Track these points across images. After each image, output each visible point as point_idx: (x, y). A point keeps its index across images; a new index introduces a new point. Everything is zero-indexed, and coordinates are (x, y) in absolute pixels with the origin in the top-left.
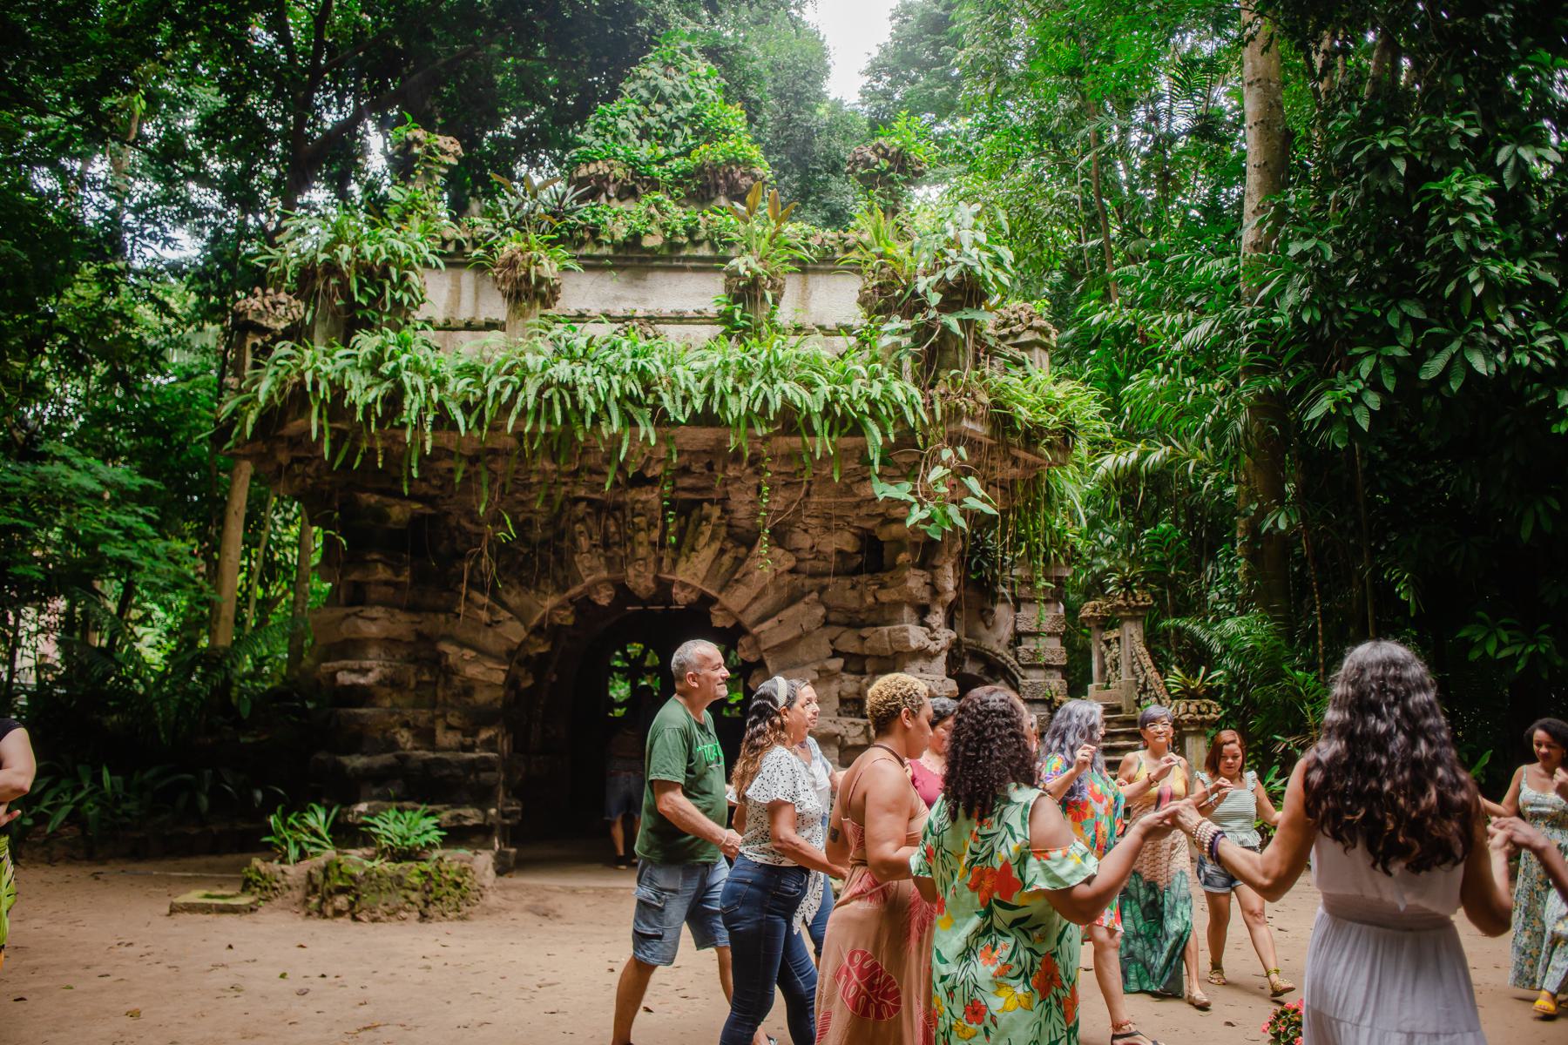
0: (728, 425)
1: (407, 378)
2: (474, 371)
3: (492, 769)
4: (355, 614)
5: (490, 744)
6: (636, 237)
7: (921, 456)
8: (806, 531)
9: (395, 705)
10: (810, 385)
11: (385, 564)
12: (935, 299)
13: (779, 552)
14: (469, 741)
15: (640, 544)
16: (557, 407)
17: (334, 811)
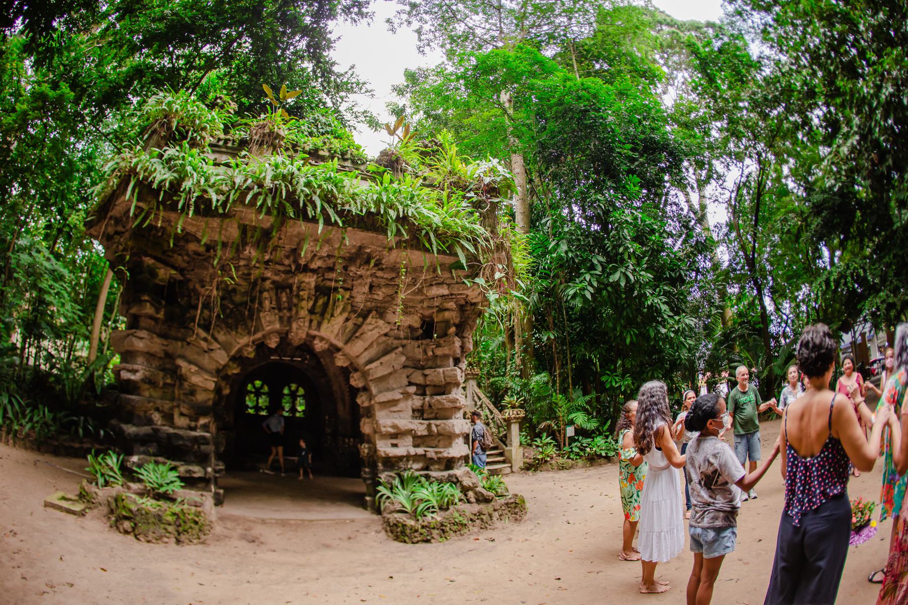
3: (207, 444)
4: (132, 334)
5: (205, 427)
9: (151, 396)
11: (152, 304)
13: (381, 322)
14: (193, 424)
15: (302, 308)
17: (121, 457)
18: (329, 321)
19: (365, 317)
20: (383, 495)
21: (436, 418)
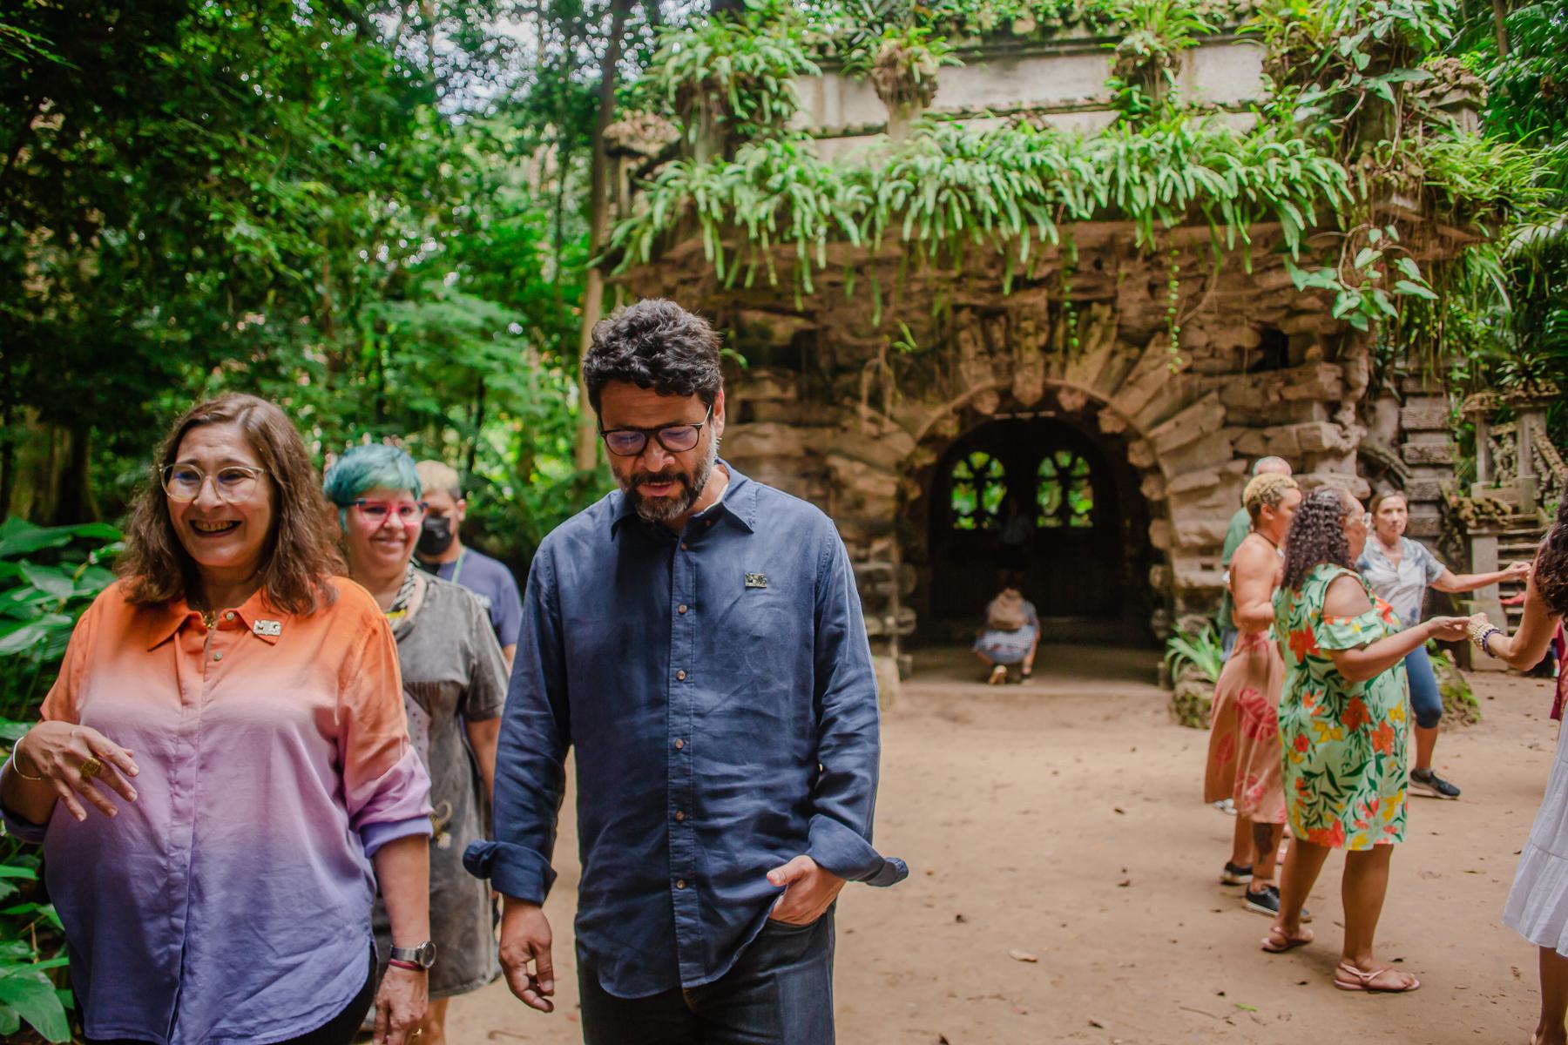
0: (1134, 218)
1: (797, 190)
2: (862, 179)
5: (883, 555)
6: (1006, 24)
7: (1341, 239)
8: (1201, 328)
10: (1220, 168)
11: (774, 381)
12: (1363, 61)
14: (862, 553)
15: (1028, 349)
16: (956, 210)
18: (1078, 362)
19: (1143, 345)
20: (1177, 655)
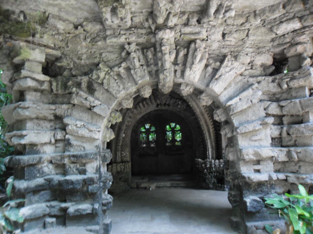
18: (191, 68)
21: (295, 145)
